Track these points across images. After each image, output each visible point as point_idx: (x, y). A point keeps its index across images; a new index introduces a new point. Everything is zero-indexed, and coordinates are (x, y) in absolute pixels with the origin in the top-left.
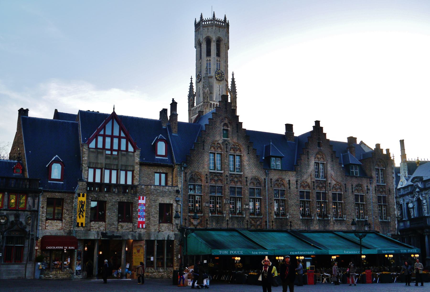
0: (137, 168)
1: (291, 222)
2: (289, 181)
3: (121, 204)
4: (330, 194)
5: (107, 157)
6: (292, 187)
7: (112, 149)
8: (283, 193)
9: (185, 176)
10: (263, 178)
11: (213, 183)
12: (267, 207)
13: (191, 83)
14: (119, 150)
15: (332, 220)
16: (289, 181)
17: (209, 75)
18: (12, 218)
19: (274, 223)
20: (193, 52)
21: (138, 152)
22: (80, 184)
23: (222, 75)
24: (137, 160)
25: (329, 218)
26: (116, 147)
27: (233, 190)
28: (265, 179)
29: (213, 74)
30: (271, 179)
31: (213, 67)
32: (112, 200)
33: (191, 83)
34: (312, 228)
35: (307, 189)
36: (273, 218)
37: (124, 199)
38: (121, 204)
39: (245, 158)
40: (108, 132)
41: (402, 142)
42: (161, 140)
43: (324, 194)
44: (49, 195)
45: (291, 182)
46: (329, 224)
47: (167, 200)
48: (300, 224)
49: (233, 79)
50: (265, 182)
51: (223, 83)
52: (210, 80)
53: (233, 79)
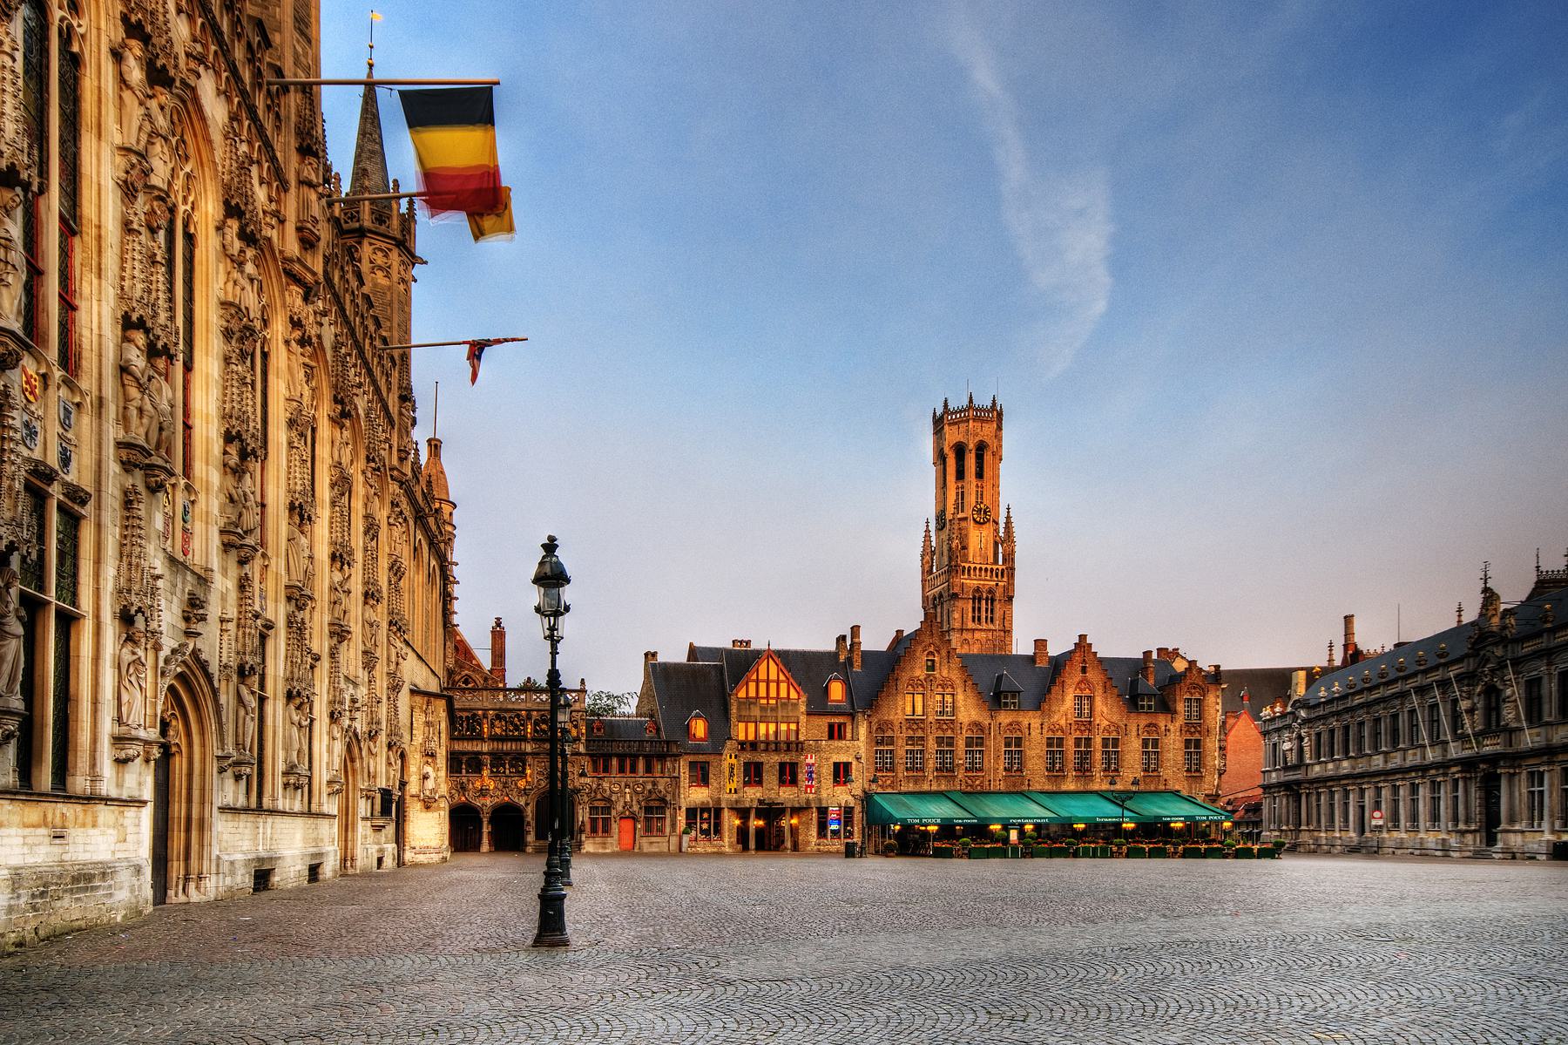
0: (803, 719)
3: (782, 765)
4: (1098, 741)
5: (763, 708)
7: (768, 697)
8: (1019, 742)
9: (870, 726)
11: (911, 733)
13: (928, 531)
14: (778, 697)
17: (960, 515)
18: (649, 787)
20: (931, 472)
21: (804, 699)
22: (728, 743)
23: (985, 515)
24: (803, 708)
26: (773, 693)
27: (939, 741)
29: (968, 513)
31: (971, 499)
32: (771, 760)
33: (928, 531)
35: (1059, 734)
37: (787, 759)
38: (782, 765)
39: (960, 697)
40: (763, 676)
41: (1348, 620)
42: (836, 679)
43: (1088, 740)
44: (691, 758)
47: (843, 758)
49: (1008, 517)
51: (987, 532)
52: (963, 524)
53: (1008, 517)
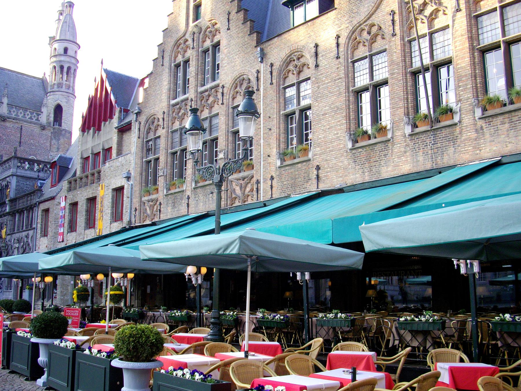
1: (318, 168)
2: (317, 46)
6: (322, 61)
10: (254, 71)
12: (262, 141)
15: (467, 120)
16: (317, 46)
19: (275, 182)
25: (456, 119)
28: (258, 72)
30: (272, 65)
34: (387, 172)
36: (273, 168)
45: (320, 49)
46: (454, 140)
48: (345, 169)
50: (258, 79)
